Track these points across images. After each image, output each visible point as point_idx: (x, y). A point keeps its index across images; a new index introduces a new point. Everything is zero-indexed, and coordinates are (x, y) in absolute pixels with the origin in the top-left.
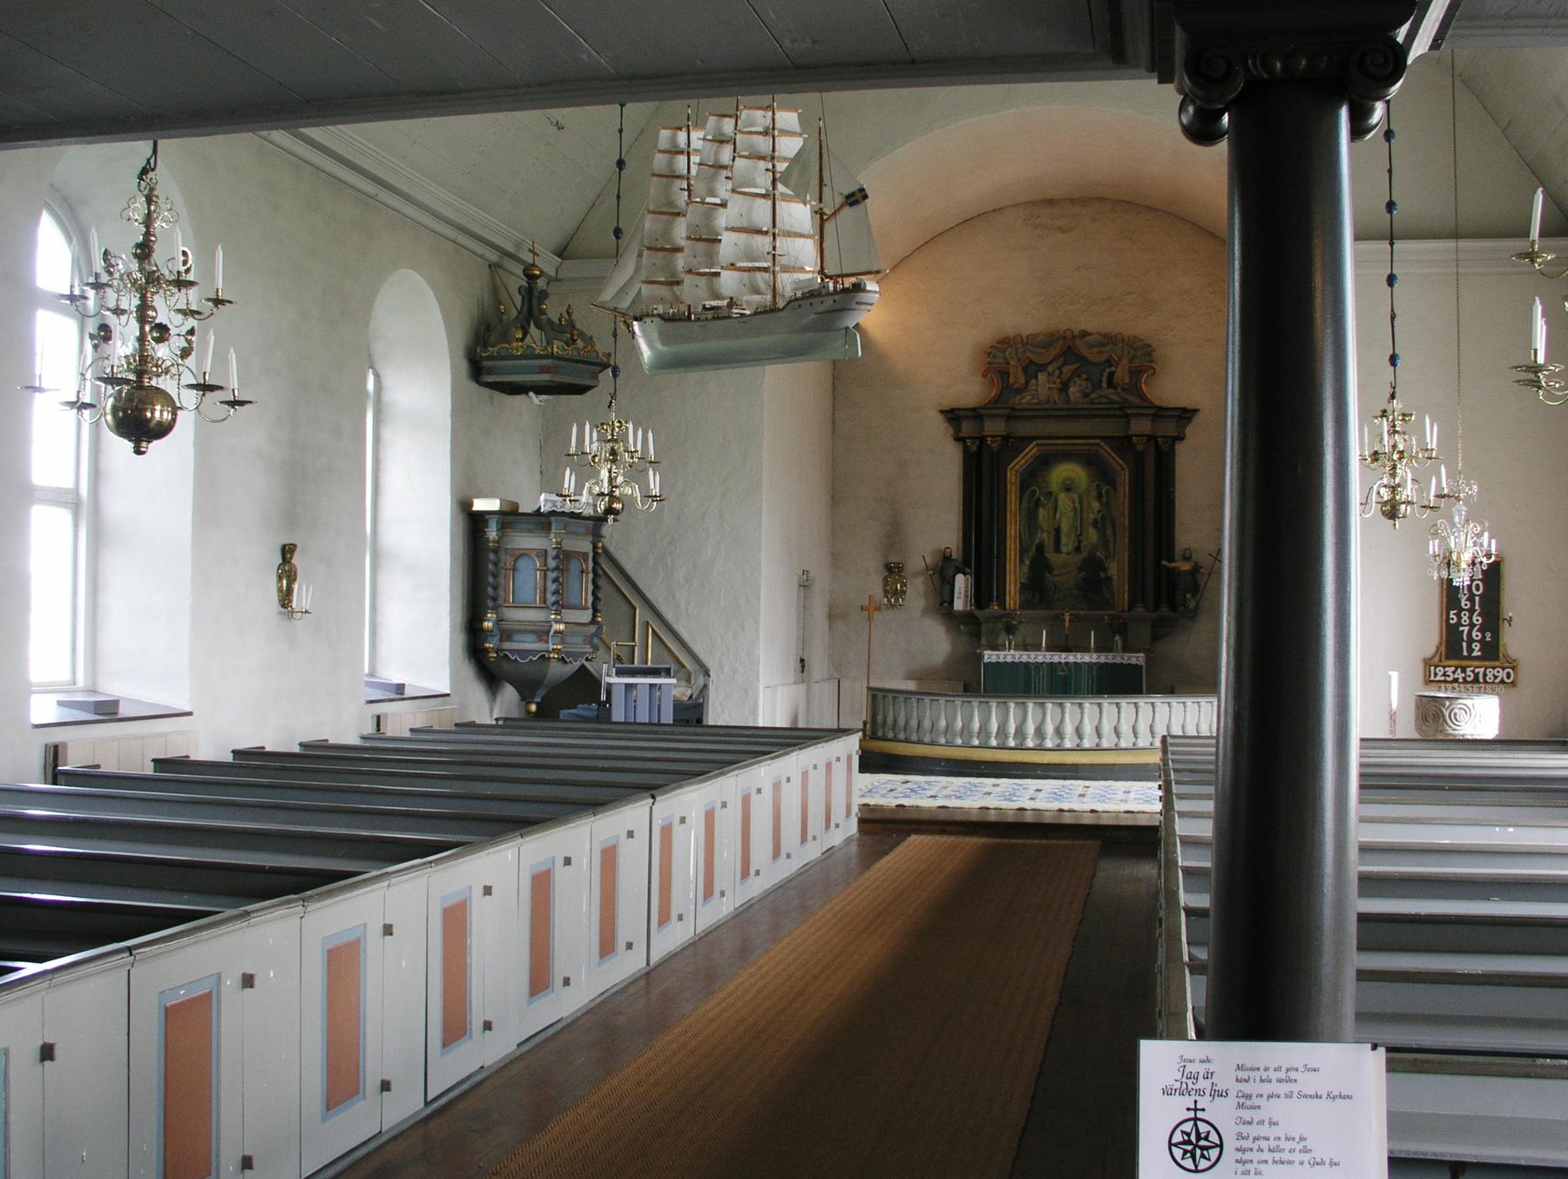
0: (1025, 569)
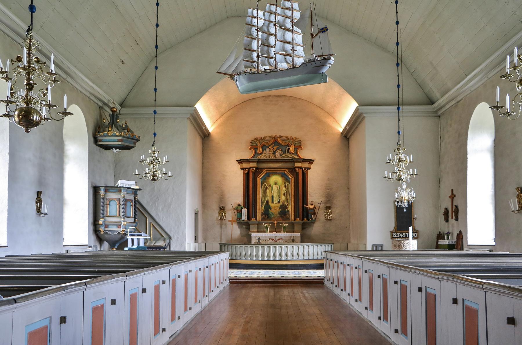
0: (263, 208)
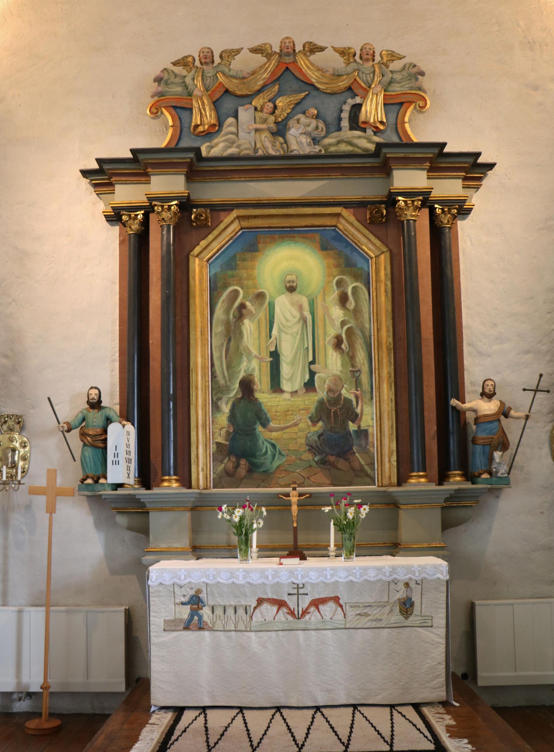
0: (223, 419)
